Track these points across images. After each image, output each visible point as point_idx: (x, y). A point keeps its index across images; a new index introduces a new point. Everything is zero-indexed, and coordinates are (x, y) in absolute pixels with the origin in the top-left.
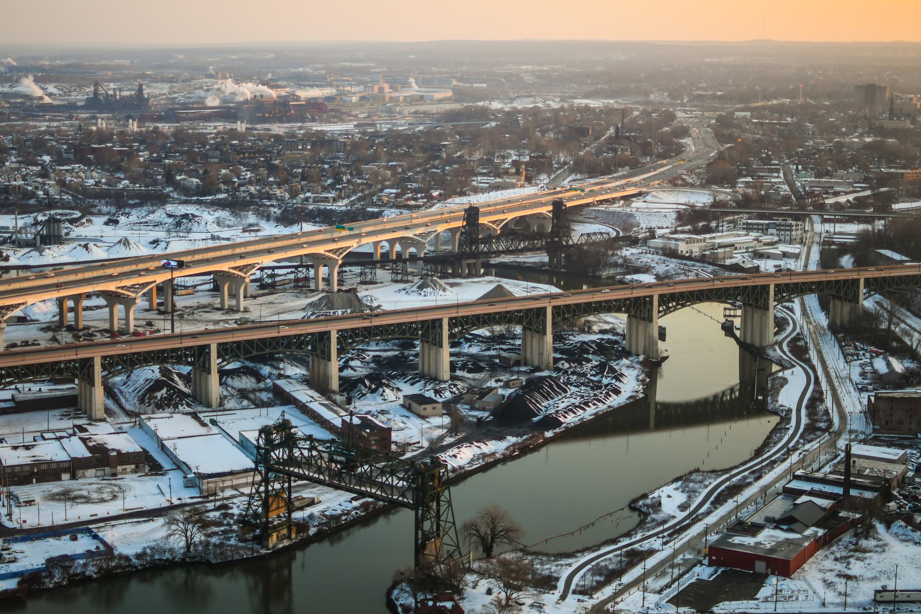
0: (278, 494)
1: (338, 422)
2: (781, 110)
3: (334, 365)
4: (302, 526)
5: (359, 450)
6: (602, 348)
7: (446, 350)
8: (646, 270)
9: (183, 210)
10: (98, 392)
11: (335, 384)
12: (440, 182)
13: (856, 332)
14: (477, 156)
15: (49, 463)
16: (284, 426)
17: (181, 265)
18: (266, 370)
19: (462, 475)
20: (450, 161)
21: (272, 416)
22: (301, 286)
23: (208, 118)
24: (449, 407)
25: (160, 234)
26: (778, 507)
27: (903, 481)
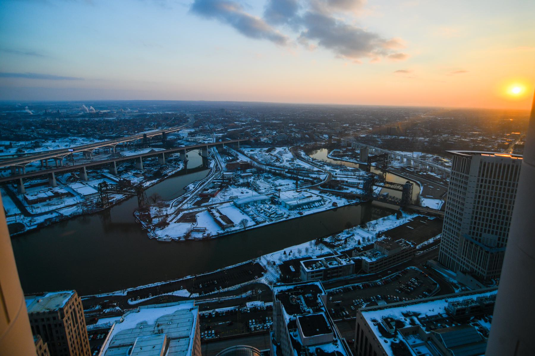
0: (105, 197)
1: (118, 180)
3: (116, 169)
4: (111, 203)
6: (175, 160)
7: (142, 163)
8: (183, 144)
10: (54, 181)
11: (116, 172)
13: (223, 153)
15: (43, 198)
16: (104, 183)
18: (99, 171)
19: (147, 188)
21: (101, 181)
22: (106, 153)
24: (143, 174)
26: (211, 185)
27: (233, 178)
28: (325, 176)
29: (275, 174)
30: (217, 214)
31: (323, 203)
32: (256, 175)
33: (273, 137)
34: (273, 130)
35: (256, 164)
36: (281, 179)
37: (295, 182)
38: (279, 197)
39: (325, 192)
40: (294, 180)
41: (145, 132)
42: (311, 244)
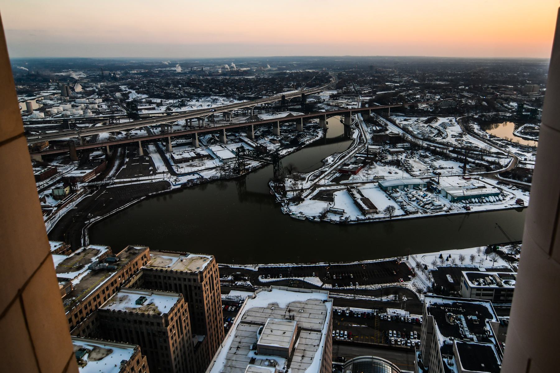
1: (255, 146)
2: (352, 72)
3: (253, 133)
4: (248, 169)
5: (260, 152)
8: (323, 109)
9: (215, 97)
10: (197, 141)
11: (253, 137)
12: (276, 90)
13: (369, 121)
14: (284, 83)
15: (186, 158)
16: (242, 147)
17: (215, 111)
18: (237, 134)
19: (284, 156)
20: (278, 85)
21: (239, 145)
22: (244, 115)
23: (220, 75)
24: (280, 141)
25: (210, 104)
26: (353, 160)
27: (379, 153)
28: (508, 160)
29: (434, 153)
30: (358, 196)
31: (501, 198)
32: (409, 152)
33: (435, 103)
34: (435, 94)
35: (410, 137)
36: (442, 159)
37: (462, 165)
38: (438, 183)
39: (506, 184)
40: (461, 162)
41: (284, 94)
42: (479, 251)
